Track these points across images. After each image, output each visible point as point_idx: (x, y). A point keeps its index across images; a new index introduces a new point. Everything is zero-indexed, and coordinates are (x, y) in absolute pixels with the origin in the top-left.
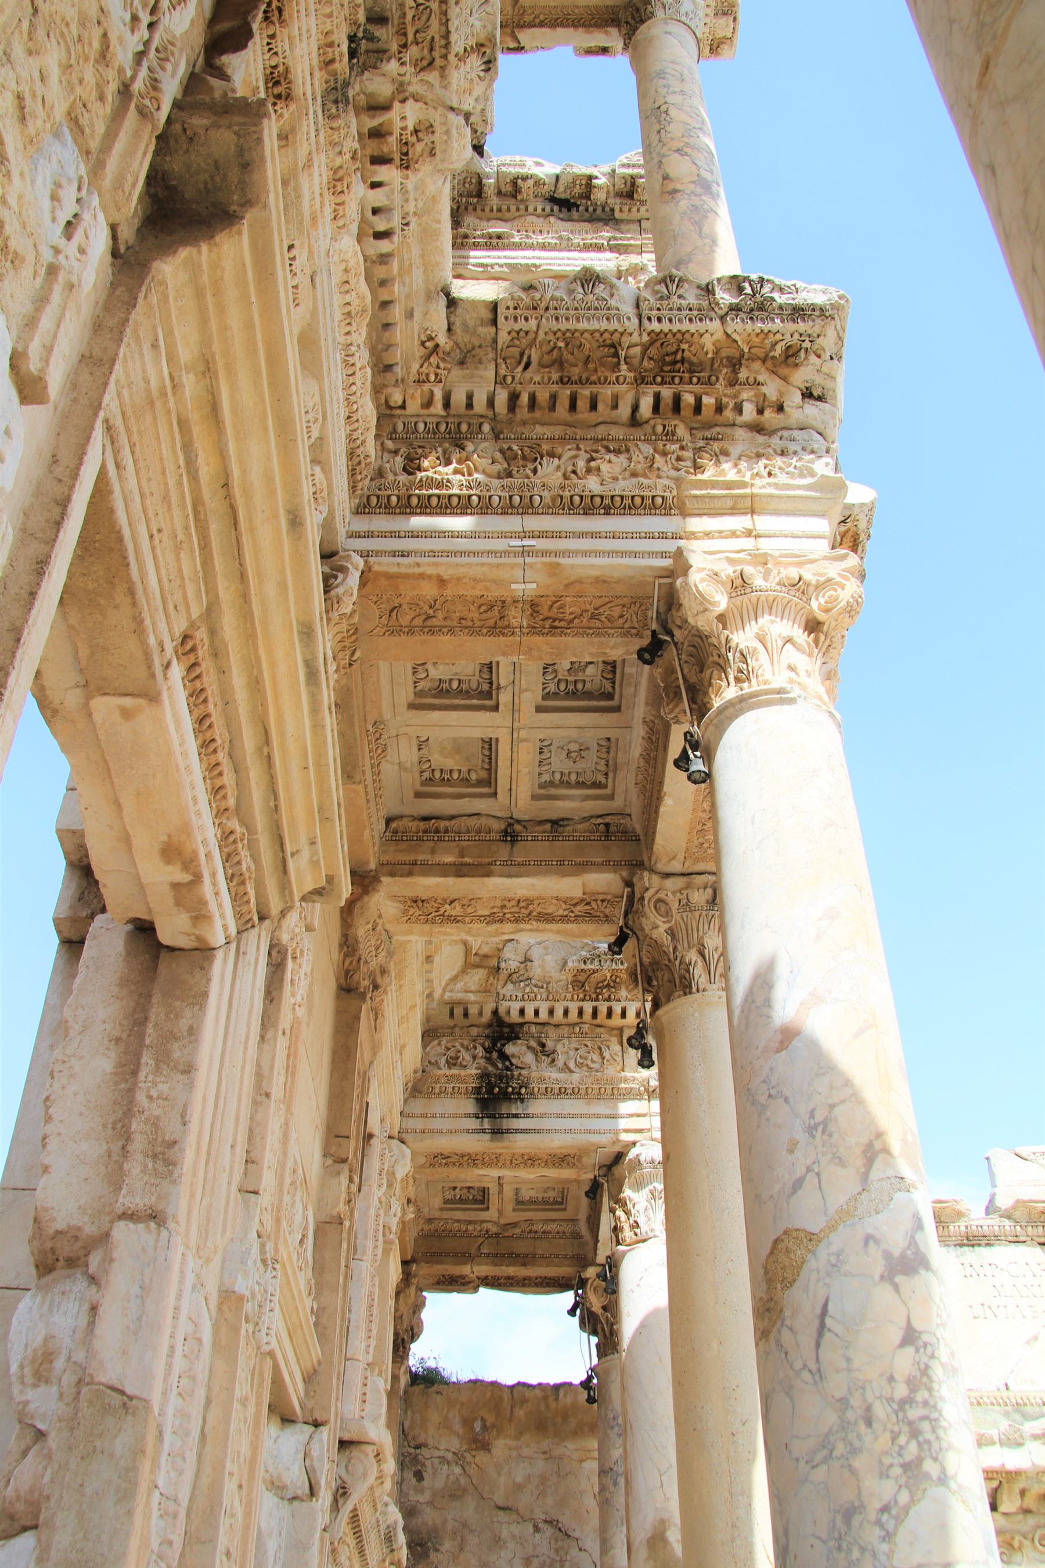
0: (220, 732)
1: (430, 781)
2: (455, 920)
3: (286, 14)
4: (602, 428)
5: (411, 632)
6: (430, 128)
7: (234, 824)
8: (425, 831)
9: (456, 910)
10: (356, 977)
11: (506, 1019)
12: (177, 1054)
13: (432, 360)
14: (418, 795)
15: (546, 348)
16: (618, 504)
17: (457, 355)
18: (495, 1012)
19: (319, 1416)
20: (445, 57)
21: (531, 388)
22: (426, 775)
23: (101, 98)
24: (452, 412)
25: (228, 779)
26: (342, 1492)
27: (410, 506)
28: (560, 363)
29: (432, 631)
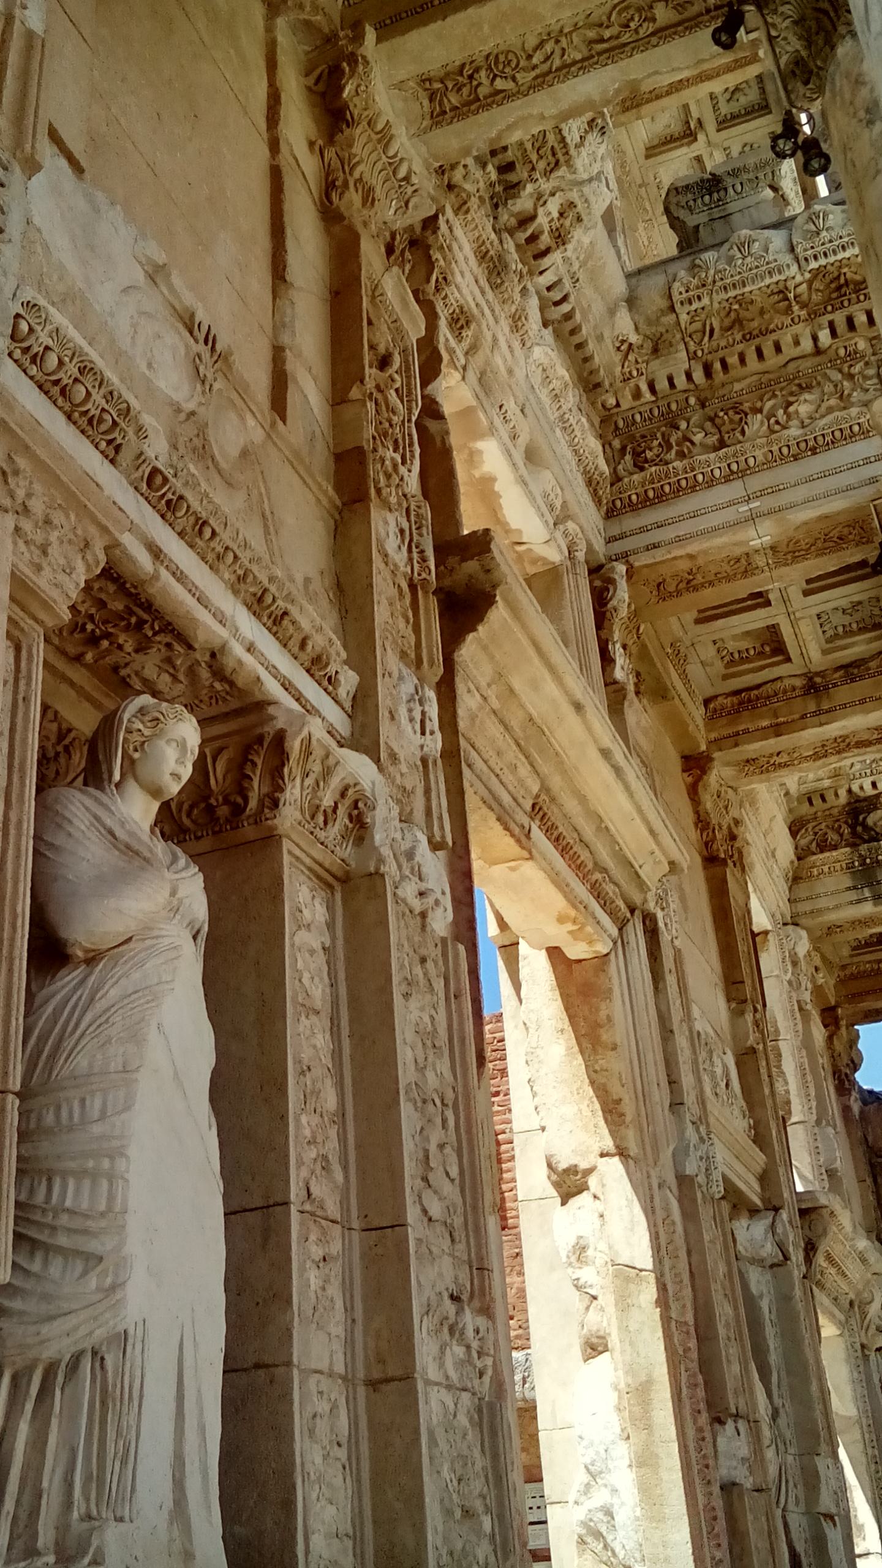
0: (570, 838)
1: (732, 663)
2: (786, 765)
3: (449, 278)
4: (792, 367)
5: (679, 593)
6: (572, 205)
7: (597, 876)
8: (740, 703)
9: (784, 758)
10: (715, 847)
11: (862, 794)
12: (604, 1037)
13: (630, 357)
14: (725, 677)
15: (723, 314)
16: (821, 443)
17: (649, 345)
18: (850, 791)
19: (775, 1203)
20: (567, 153)
21: (721, 354)
22: (727, 659)
23: (408, 622)
24: (660, 396)
25: (584, 855)
26: (810, 1248)
27: (649, 500)
28: (739, 322)
29: (696, 589)
